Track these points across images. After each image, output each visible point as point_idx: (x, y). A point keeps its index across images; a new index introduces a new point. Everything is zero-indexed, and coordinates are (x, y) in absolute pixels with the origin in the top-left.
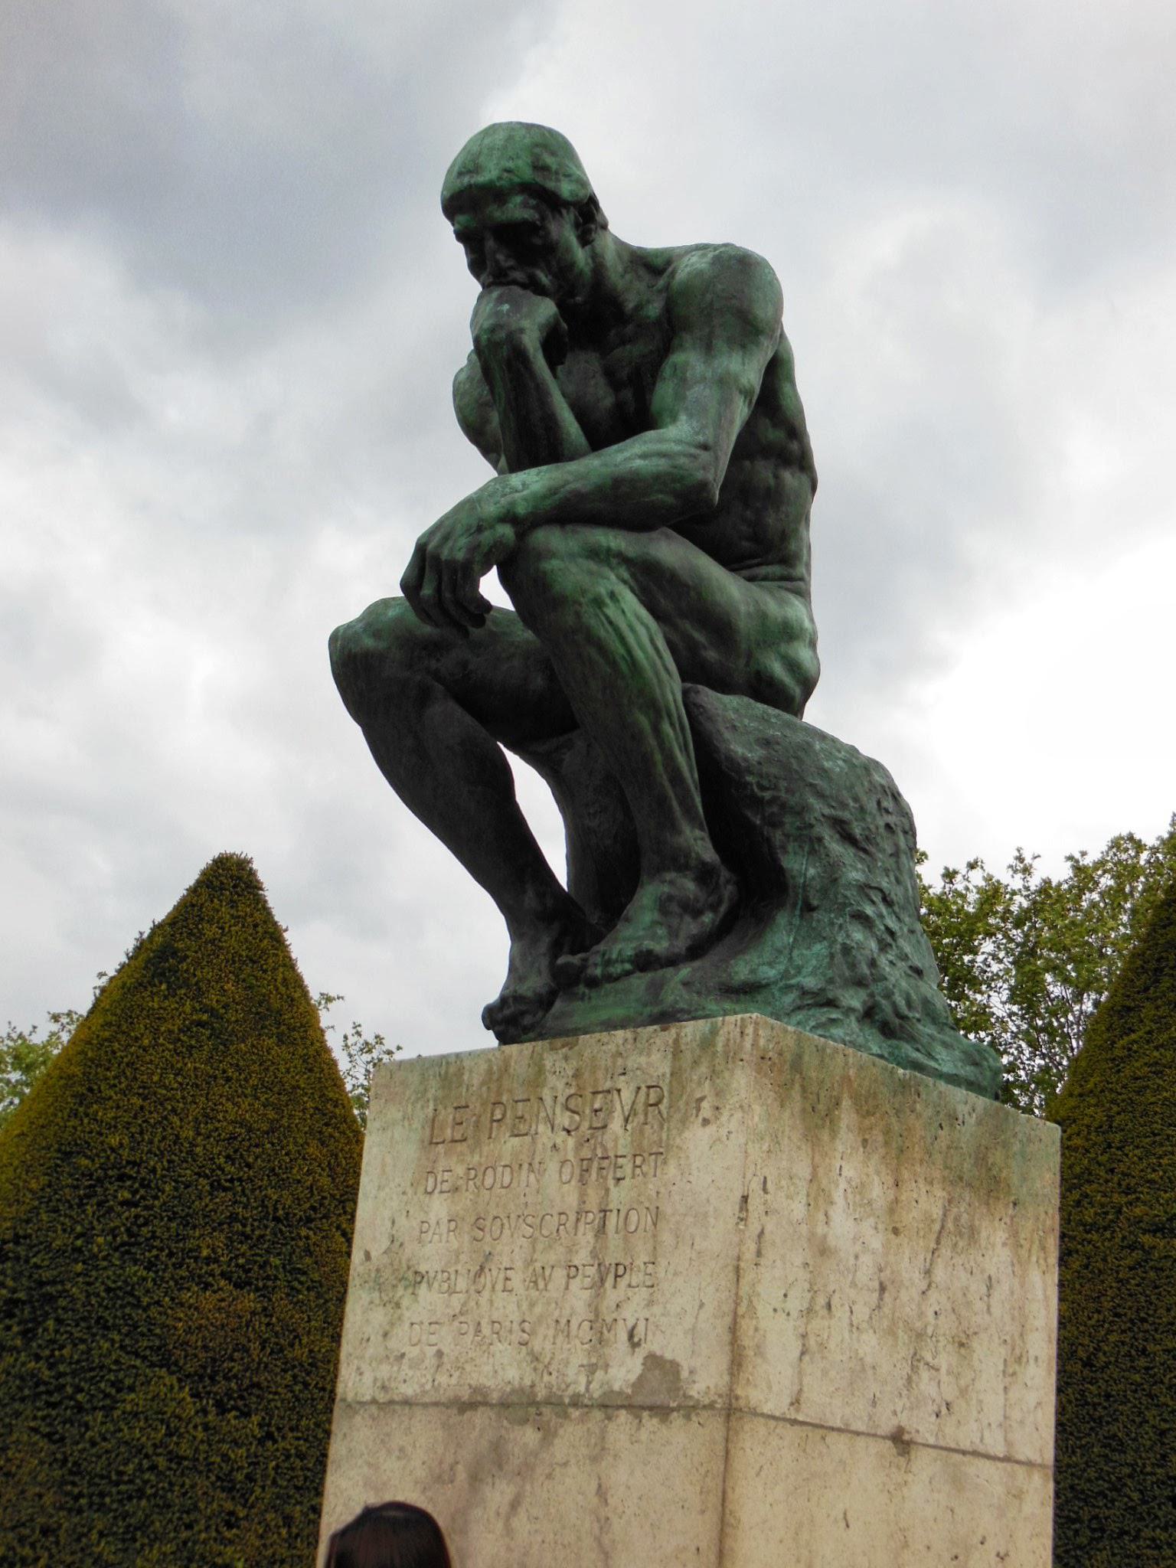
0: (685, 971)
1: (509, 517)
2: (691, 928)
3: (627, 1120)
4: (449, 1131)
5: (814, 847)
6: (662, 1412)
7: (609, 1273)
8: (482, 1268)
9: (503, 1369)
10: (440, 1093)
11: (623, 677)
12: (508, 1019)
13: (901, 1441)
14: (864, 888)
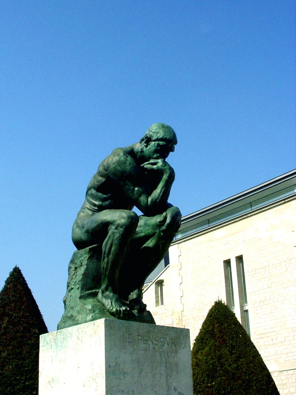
4: (128, 339)
7: (168, 376)
8: (141, 372)
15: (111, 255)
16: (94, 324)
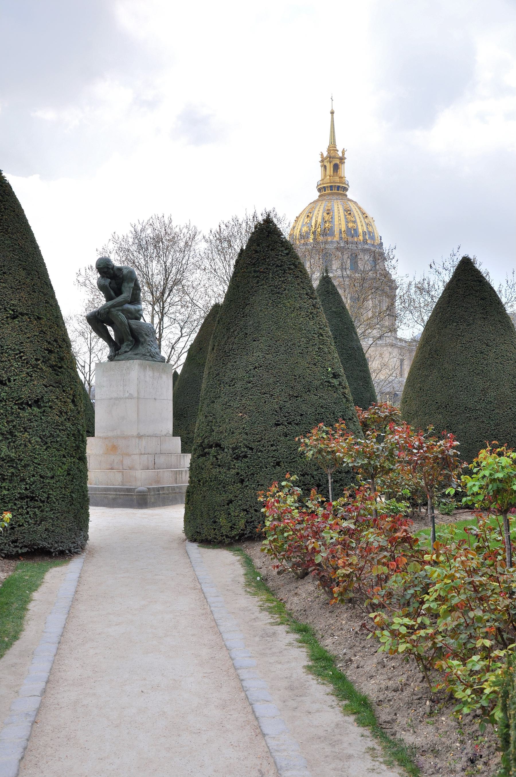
0: (129, 353)
1: (108, 308)
2: (130, 347)
5: (143, 337)
6: (131, 399)
9: (114, 395)
11: (122, 323)
12: (111, 358)
13: (155, 399)
14: (149, 341)
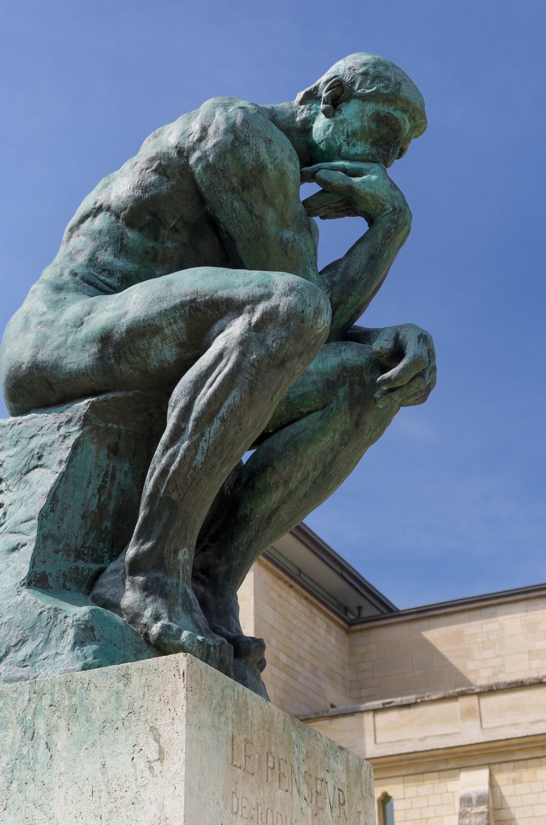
3: (331, 809)
10: (234, 716)
15: (217, 423)
16: (127, 677)
